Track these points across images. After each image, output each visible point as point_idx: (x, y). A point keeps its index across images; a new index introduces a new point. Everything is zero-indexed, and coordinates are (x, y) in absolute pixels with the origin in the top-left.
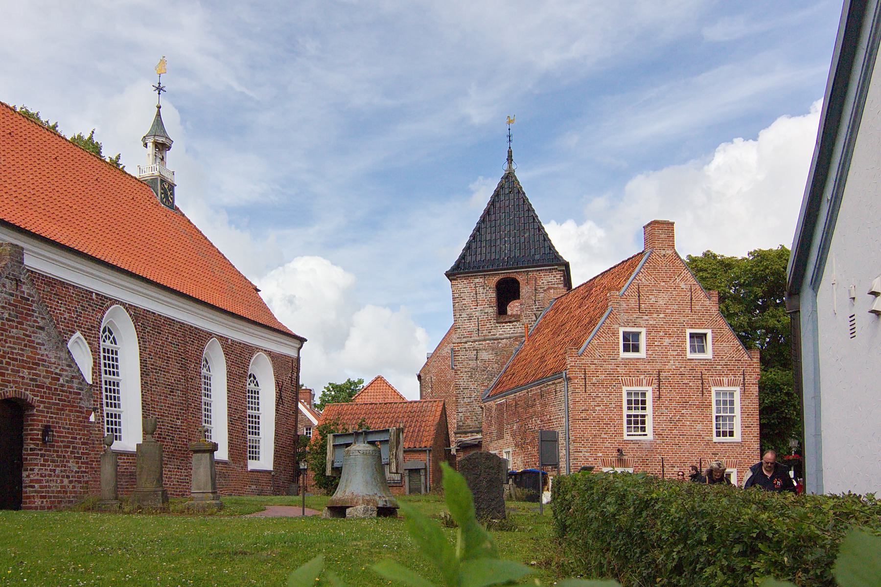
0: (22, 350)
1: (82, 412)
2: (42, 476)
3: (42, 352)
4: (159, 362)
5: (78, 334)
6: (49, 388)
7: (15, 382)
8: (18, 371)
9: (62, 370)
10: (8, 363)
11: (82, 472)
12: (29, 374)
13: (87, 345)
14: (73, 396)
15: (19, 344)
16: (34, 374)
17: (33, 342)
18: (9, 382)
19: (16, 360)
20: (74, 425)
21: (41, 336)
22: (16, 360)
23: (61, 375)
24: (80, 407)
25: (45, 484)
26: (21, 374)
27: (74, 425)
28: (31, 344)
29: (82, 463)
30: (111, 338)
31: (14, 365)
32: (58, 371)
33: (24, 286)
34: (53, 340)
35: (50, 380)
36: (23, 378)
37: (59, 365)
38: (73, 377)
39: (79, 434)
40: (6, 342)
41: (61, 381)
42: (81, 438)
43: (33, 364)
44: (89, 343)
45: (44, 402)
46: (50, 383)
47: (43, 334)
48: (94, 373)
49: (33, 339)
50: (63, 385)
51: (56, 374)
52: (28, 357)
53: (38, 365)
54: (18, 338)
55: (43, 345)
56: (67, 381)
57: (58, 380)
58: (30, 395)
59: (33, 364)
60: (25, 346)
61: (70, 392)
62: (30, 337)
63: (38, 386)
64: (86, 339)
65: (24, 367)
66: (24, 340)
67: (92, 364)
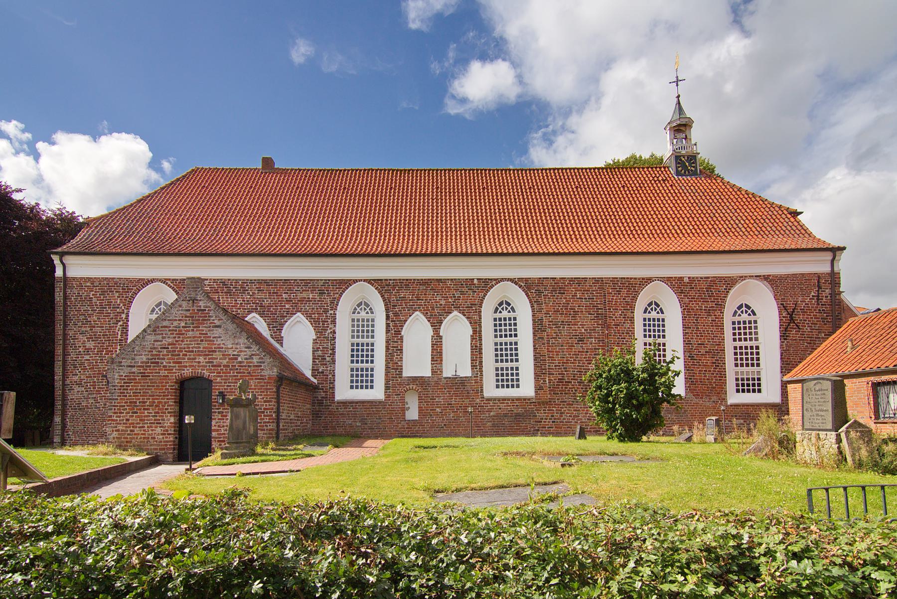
0: (198, 344)
1: (263, 379)
2: (219, 426)
3: (217, 343)
4: (560, 318)
5: (455, 313)
6: (224, 366)
7: (193, 366)
8: (195, 359)
9: (241, 351)
10: (186, 355)
11: (264, 422)
12: (205, 359)
13: (466, 320)
14: (252, 368)
15: (195, 341)
16: (209, 359)
17: (210, 337)
18: (186, 367)
19: (192, 351)
20: (255, 389)
21: (218, 332)
22: (192, 351)
23: (239, 355)
24: (261, 376)
25: (223, 432)
26: (197, 360)
27: (255, 389)
28: (207, 338)
29: (264, 416)
30: (509, 308)
31: (190, 355)
32: (235, 353)
33: (201, 302)
34: (230, 333)
35: (227, 360)
36: (199, 362)
37: (237, 348)
38: (253, 355)
39: (261, 395)
40: (182, 341)
41: (240, 359)
42: (263, 398)
43: (209, 351)
44: (467, 318)
45: (222, 376)
46: (227, 362)
47: (220, 330)
48: (473, 338)
49: (209, 335)
50: (240, 362)
51: (233, 355)
52: (204, 348)
53: (216, 351)
54: (194, 337)
55: (220, 337)
56: (246, 359)
57: (236, 359)
58: (206, 373)
59: (209, 351)
60: (202, 341)
61: (249, 366)
62: (207, 334)
63: (212, 366)
64: (464, 315)
65: (200, 355)
66: (200, 337)
67: (471, 333)
